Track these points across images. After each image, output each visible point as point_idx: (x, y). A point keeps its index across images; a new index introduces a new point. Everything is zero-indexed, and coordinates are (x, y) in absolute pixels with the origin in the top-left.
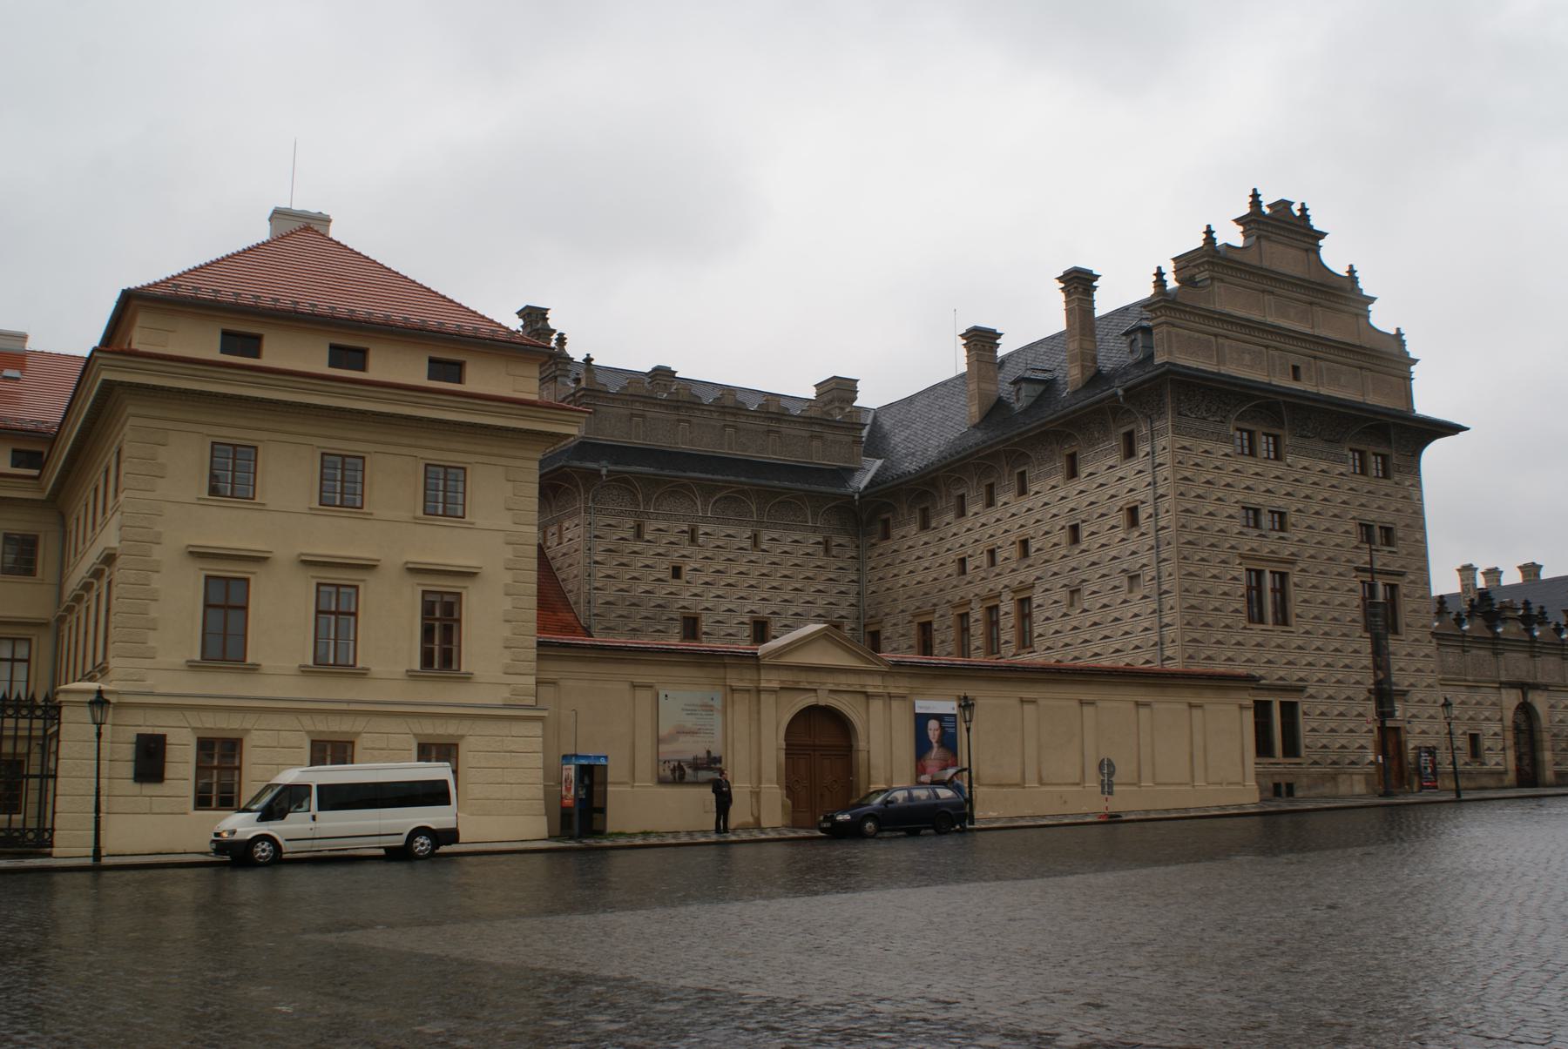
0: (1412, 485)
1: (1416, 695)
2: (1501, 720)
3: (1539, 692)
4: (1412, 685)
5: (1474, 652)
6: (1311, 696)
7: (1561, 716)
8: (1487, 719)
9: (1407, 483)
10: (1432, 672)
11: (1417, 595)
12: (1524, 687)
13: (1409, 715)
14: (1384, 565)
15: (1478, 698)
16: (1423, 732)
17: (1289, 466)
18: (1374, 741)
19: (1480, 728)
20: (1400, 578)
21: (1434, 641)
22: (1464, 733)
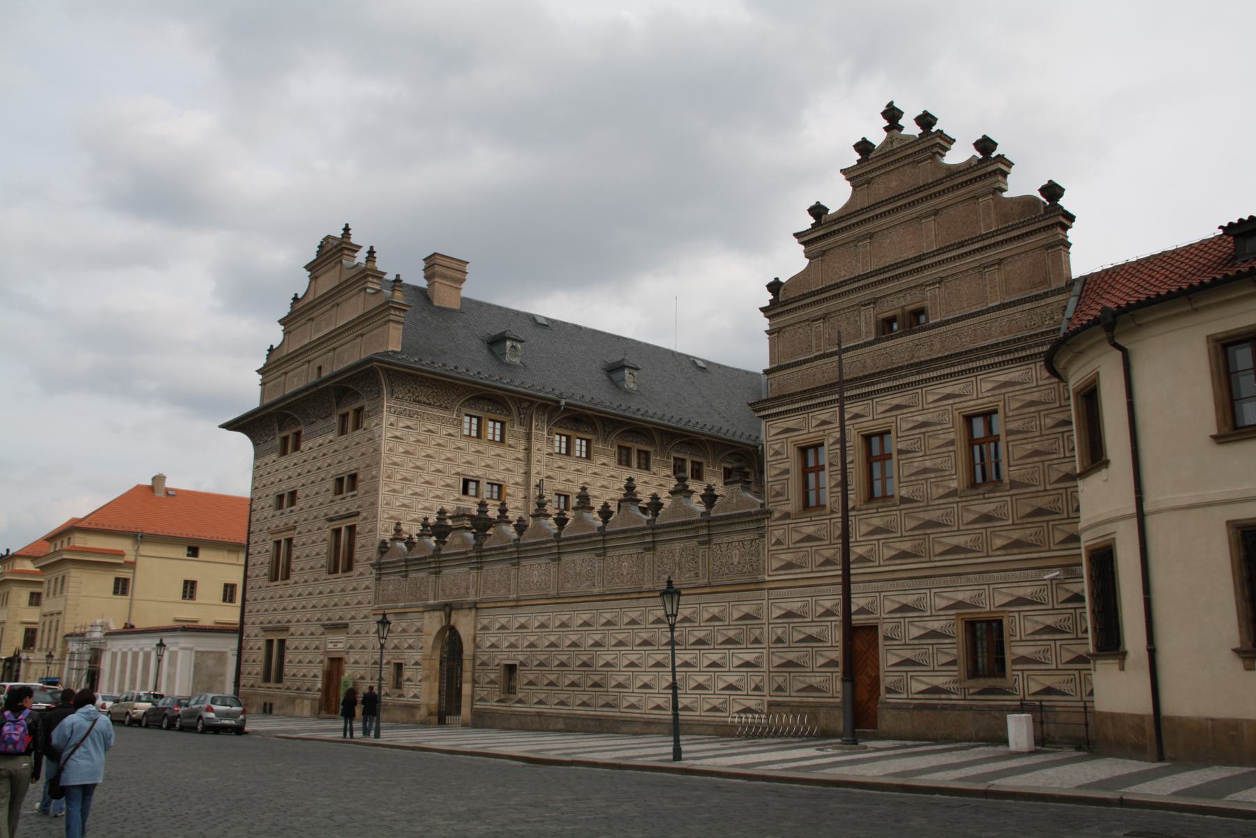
0: (377, 425)
1: (354, 627)
2: (421, 648)
3: (466, 612)
4: (353, 618)
5: (412, 575)
6: (292, 634)
7: (493, 640)
8: (410, 647)
9: (373, 425)
10: (369, 603)
11: (367, 530)
12: (448, 609)
13: (348, 646)
14: (348, 509)
15: (404, 625)
16: (356, 662)
17: (302, 452)
18: (323, 671)
19: (402, 657)
20: (356, 518)
21: (374, 571)
22: (388, 663)
